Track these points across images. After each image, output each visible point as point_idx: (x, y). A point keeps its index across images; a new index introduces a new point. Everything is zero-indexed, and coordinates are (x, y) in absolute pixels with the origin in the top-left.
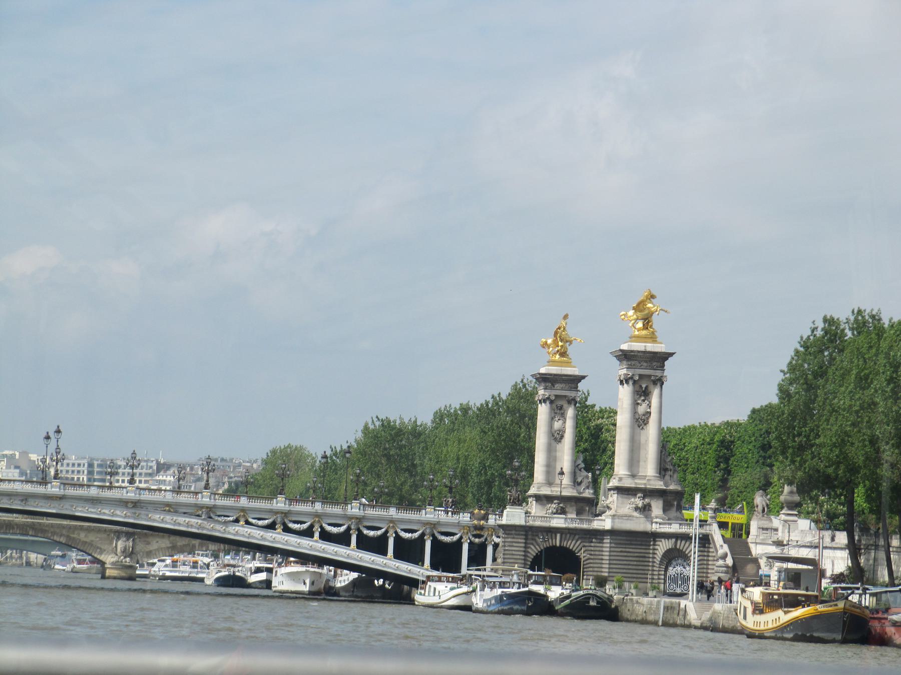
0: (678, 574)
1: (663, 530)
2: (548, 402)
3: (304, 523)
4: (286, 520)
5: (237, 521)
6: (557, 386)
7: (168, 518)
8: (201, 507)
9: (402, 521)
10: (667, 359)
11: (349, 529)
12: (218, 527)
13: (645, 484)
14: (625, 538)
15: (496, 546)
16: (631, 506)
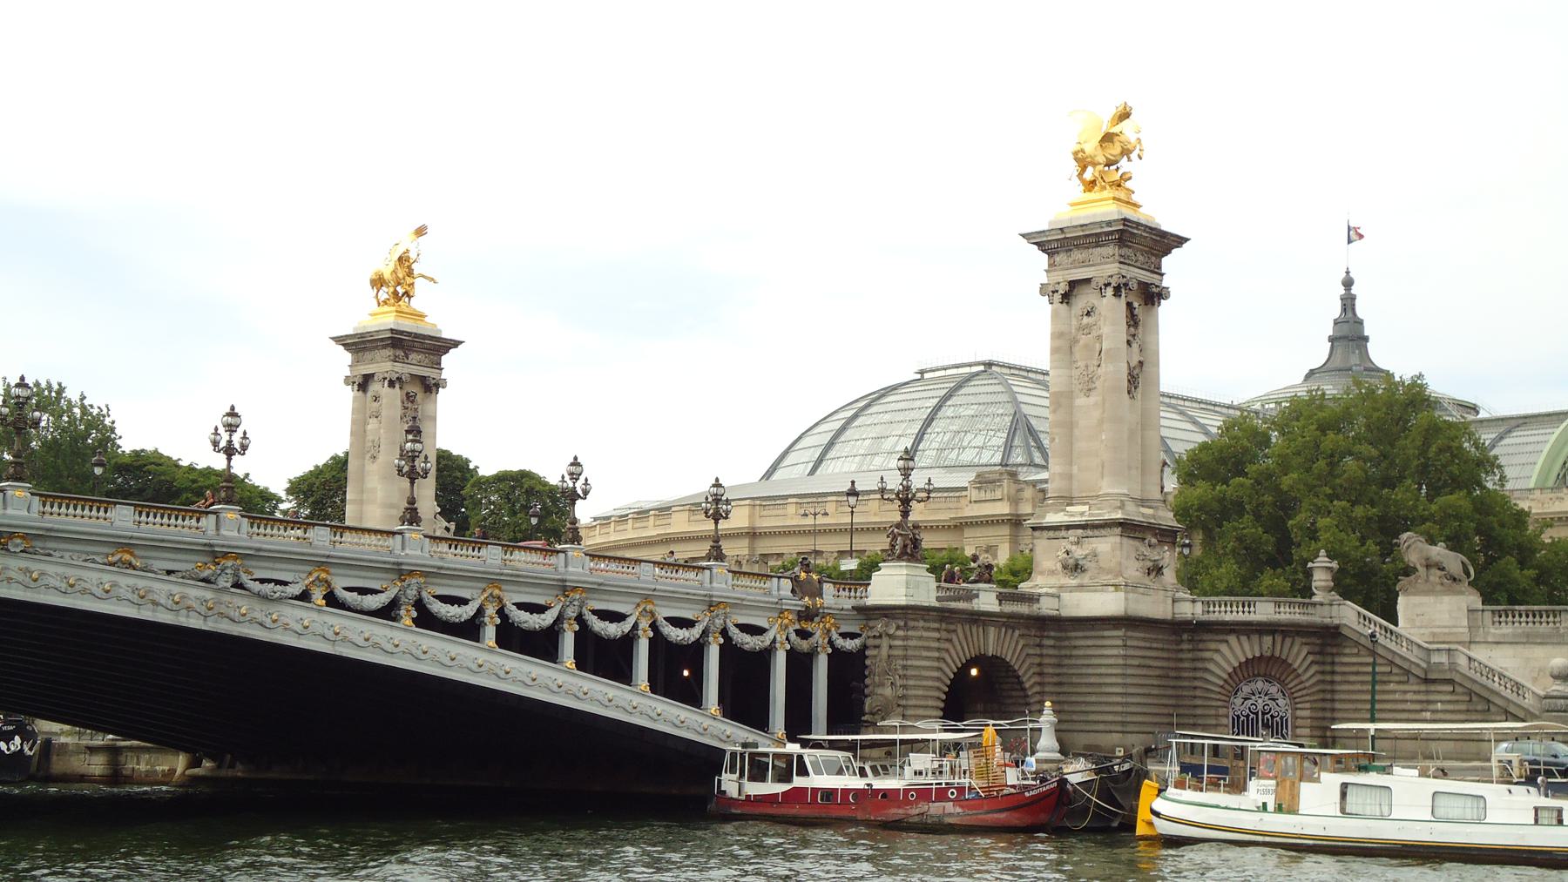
0: (1257, 714)
1: (1228, 617)
2: (397, 386)
3: (462, 602)
4: (424, 594)
5: (305, 596)
6: (414, 357)
7: (126, 581)
8: (215, 554)
9: (670, 598)
10: (1167, 252)
11: (560, 619)
12: (259, 611)
13: (1154, 516)
14: (1142, 635)
15: (837, 657)
16: (1141, 564)
